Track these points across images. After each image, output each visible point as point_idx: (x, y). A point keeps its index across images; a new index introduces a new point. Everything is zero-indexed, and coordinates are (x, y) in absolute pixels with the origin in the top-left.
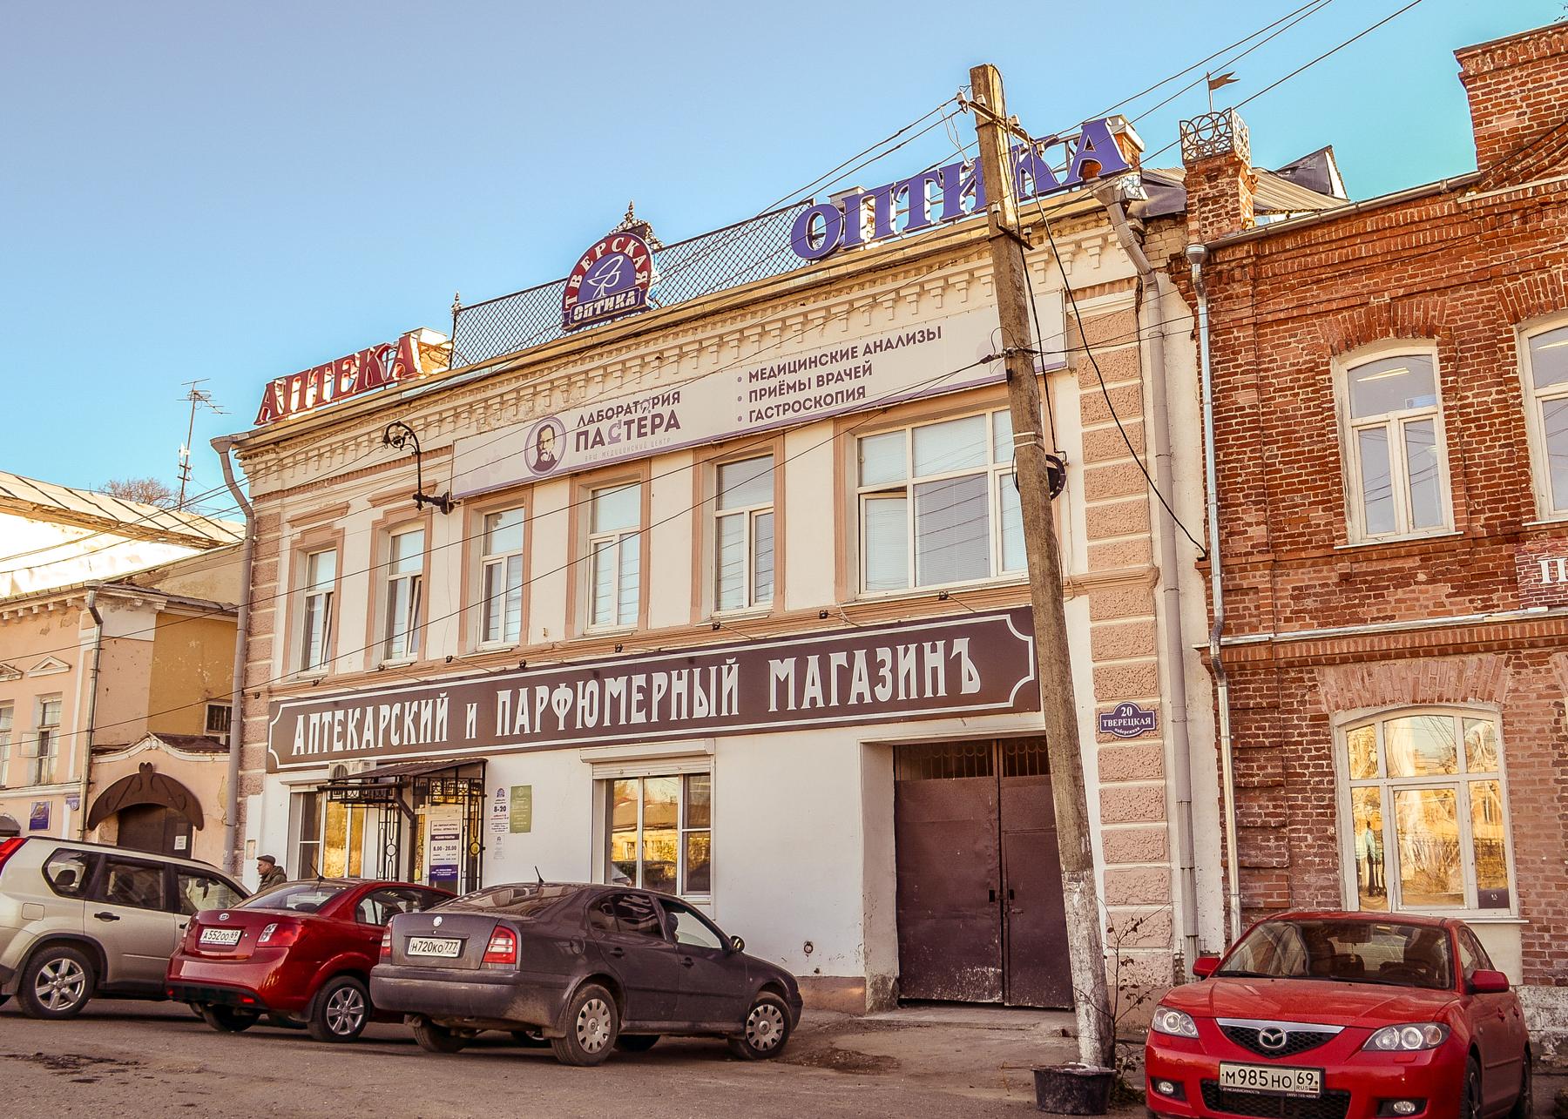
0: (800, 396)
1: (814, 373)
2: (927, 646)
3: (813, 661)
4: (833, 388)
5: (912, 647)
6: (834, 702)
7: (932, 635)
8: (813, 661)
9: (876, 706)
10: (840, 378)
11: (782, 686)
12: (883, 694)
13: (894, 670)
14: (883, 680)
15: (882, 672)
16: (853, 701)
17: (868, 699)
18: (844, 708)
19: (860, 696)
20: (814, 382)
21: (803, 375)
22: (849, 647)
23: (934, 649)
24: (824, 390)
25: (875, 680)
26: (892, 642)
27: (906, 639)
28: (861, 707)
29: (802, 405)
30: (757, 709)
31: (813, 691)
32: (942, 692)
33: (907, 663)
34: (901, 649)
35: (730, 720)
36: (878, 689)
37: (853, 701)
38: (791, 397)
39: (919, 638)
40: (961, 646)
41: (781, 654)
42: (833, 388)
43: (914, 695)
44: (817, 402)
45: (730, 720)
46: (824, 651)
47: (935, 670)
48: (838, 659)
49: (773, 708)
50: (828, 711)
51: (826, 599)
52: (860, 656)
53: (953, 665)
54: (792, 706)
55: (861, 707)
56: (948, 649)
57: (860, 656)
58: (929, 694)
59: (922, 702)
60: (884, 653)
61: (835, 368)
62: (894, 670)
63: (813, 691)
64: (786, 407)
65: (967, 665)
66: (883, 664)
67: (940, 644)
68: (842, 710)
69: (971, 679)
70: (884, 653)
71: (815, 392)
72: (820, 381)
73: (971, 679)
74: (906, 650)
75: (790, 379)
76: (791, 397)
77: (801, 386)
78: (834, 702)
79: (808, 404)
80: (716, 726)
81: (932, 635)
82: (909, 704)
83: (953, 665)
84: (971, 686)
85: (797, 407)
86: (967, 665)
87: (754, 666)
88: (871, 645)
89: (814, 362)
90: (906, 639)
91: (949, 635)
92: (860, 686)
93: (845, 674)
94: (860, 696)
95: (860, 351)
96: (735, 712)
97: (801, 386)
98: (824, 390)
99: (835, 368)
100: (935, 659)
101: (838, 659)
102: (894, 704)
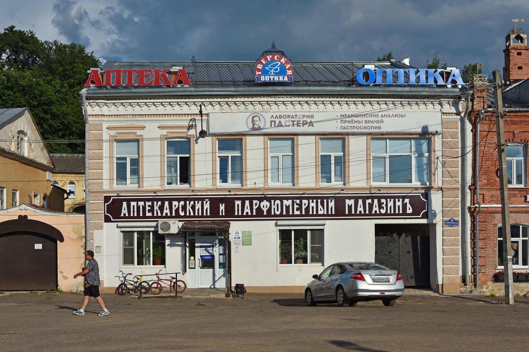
0: (360, 125)
3: (360, 202)
4: (370, 125)
5: (392, 200)
6: (367, 212)
7: (399, 197)
8: (360, 202)
9: (381, 214)
10: (372, 122)
11: (350, 207)
12: (383, 211)
13: (387, 205)
14: (383, 208)
15: (383, 205)
16: (373, 212)
17: (378, 212)
18: (370, 214)
19: (376, 211)
20: (364, 122)
21: (360, 119)
22: (373, 198)
23: (399, 201)
24: (367, 125)
25: (380, 207)
26: (386, 198)
27: (390, 197)
29: (360, 128)
30: (340, 213)
31: (360, 209)
32: (401, 212)
33: (391, 204)
34: (389, 200)
35: (332, 215)
36: (381, 210)
37: (373, 212)
38: (356, 125)
39: (394, 198)
40: (407, 201)
41: (350, 198)
42: (370, 125)
43: (392, 212)
44: (365, 128)
45: (332, 215)
46: (364, 199)
47: (399, 206)
49: (347, 213)
50: (365, 215)
51: (363, 184)
52: (376, 201)
53: (404, 206)
54: (353, 212)
55: (376, 214)
56: (403, 201)
57: (376, 201)
59: (395, 214)
60: (383, 201)
61: (371, 119)
62: (387, 205)
63: (360, 209)
64: (354, 127)
65: (408, 206)
66: (383, 203)
67: (401, 200)
68: (369, 215)
70: (383, 201)
71: (364, 125)
74: (390, 201)
76: (356, 125)
77: (360, 122)
78: (367, 212)
80: (327, 216)
83: (404, 206)
84: (410, 211)
86: (408, 206)
87: (340, 201)
88: (379, 198)
89: (364, 116)
90: (390, 197)
91: (404, 198)
92: (376, 209)
93: (371, 206)
94: (376, 211)
95: (380, 116)
96: (333, 213)
97: (360, 122)
98: (367, 125)
99: (371, 119)
100: (399, 203)
101: (370, 201)
102: (386, 214)
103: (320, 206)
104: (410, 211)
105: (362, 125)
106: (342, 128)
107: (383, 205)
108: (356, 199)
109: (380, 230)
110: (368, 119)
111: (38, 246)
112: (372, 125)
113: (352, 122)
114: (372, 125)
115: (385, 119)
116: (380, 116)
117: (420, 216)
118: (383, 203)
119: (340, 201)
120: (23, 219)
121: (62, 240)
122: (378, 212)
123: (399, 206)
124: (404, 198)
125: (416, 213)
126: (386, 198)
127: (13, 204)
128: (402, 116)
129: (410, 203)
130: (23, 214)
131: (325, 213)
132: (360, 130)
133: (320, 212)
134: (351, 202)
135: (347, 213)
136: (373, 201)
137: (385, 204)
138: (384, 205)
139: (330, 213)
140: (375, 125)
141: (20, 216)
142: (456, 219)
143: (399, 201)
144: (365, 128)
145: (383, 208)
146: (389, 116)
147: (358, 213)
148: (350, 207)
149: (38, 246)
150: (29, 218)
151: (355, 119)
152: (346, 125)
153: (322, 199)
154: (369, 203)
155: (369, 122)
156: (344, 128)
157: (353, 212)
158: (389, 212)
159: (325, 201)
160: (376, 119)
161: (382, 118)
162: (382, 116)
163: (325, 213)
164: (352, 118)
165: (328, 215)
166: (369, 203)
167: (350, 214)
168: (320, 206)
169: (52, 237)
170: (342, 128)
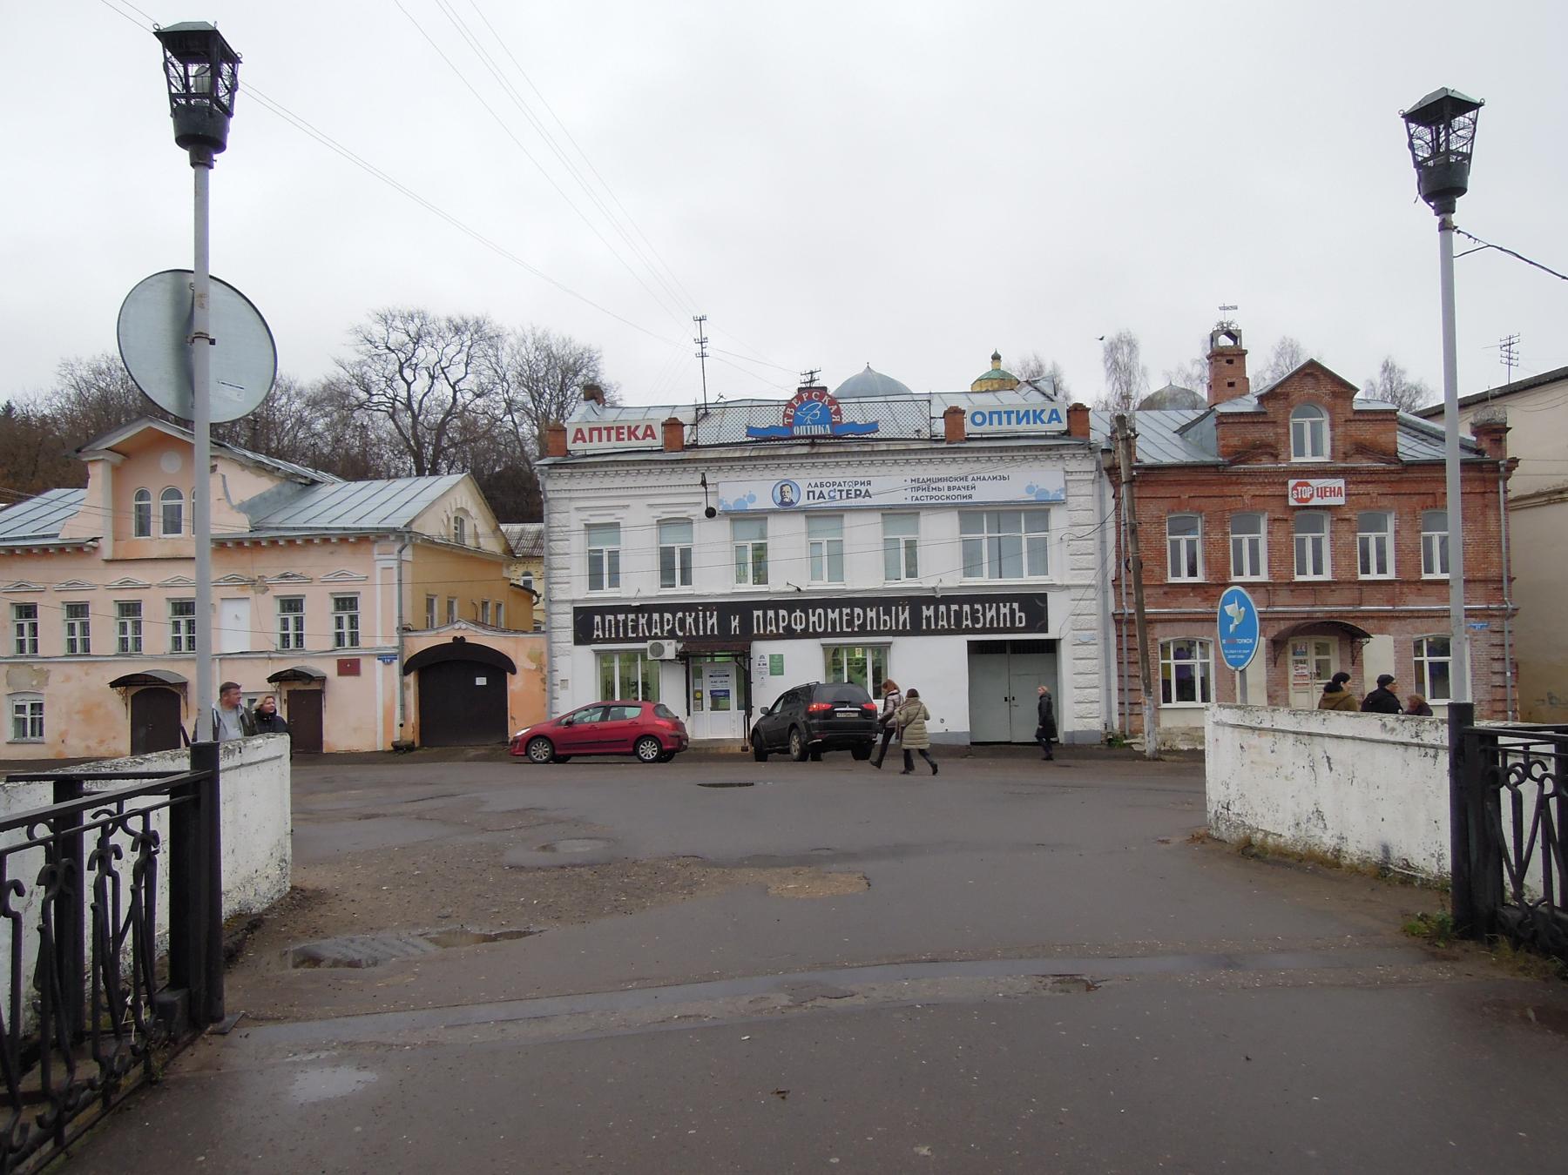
1: (946, 484)
4: (956, 492)
21: (940, 485)
24: (951, 493)
38: (934, 493)
40: (1016, 606)
42: (956, 492)
52: (966, 608)
53: (1012, 611)
62: (984, 615)
68: (959, 630)
76: (934, 493)
98: (951, 493)
100: (1005, 610)
105: (944, 494)
109: (975, 649)
111: (481, 681)
115: (977, 483)
120: (459, 641)
121: (514, 672)
127: (450, 621)
130: (459, 635)
141: (455, 638)
148: (928, 618)
149: (481, 681)
150: (469, 640)
152: (920, 493)
160: (965, 484)
169: (500, 666)
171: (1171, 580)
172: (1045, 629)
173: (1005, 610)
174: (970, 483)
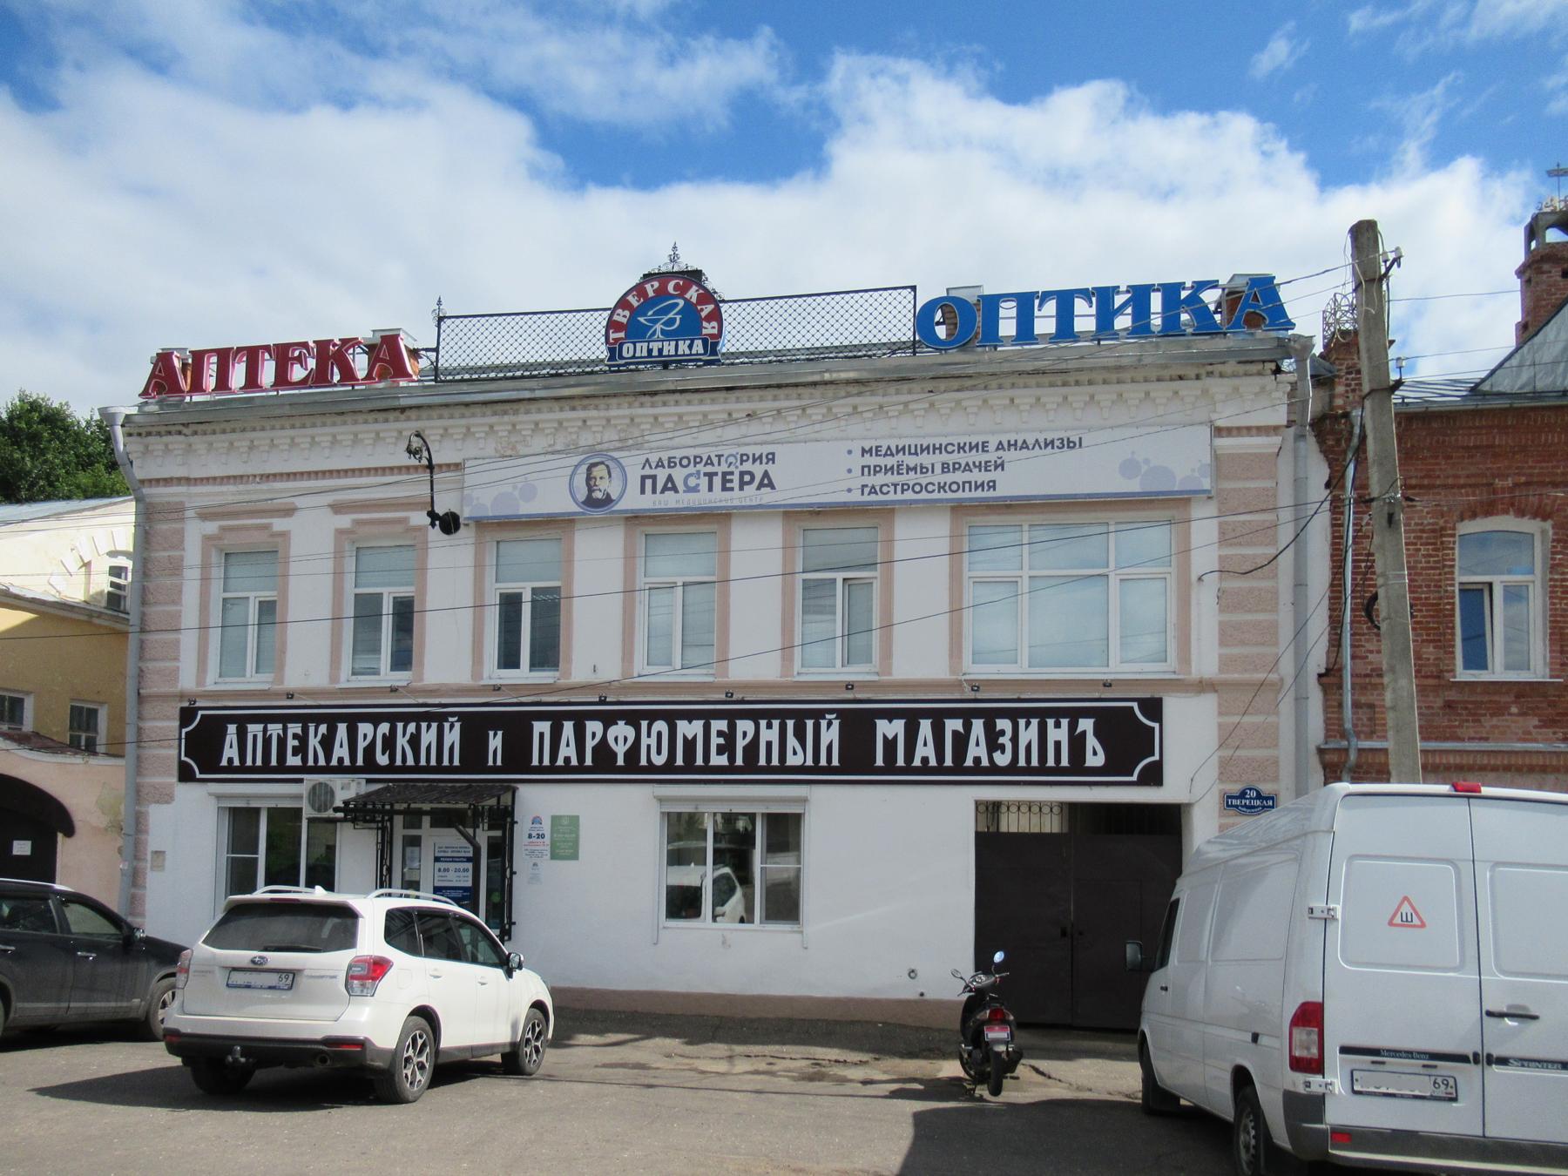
1: (938, 459)
2: (1051, 722)
3: (925, 726)
4: (959, 477)
5: (1035, 722)
6: (948, 762)
7: (1057, 714)
8: (925, 726)
9: (994, 769)
10: (967, 468)
11: (890, 745)
12: (1002, 759)
14: (1002, 748)
15: (1001, 740)
16: (969, 762)
17: (985, 763)
18: (958, 768)
19: (977, 760)
20: (938, 469)
21: (925, 459)
22: (967, 716)
23: (1058, 725)
24: (949, 478)
25: (993, 745)
26: (1013, 715)
28: (977, 768)
31: (925, 750)
32: (1065, 762)
33: (1029, 734)
34: (1022, 722)
36: (997, 756)
37: (969, 762)
38: (911, 478)
39: (1042, 714)
40: (1086, 725)
41: (890, 715)
42: (959, 477)
43: (1035, 762)
44: (941, 488)
46: (938, 718)
47: (1058, 744)
48: (953, 725)
49: (879, 762)
52: (978, 726)
53: (1077, 742)
54: (901, 762)
56: (1073, 727)
57: (978, 726)
58: (1051, 762)
59: (1042, 769)
60: (1003, 724)
61: (962, 458)
62: (1015, 740)
63: (925, 750)
64: (905, 488)
65: (1092, 742)
66: (1002, 733)
67: (1065, 722)
68: (957, 770)
69: (1095, 753)
70: (1003, 724)
72: (945, 468)
73: (1095, 753)
75: (911, 461)
76: (911, 478)
77: (923, 470)
78: (948, 762)
79: (930, 488)
81: (1057, 714)
82: (1029, 770)
83: (1077, 742)
84: (1096, 759)
85: (917, 488)
86: (1092, 742)
87: (858, 726)
88: (990, 717)
90: (1028, 714)
91: (1074, 715)
92: (977, 750)
93: (961, 741)
94: (977, 760)
97: (923, 470)
98: (949, 478)
99: (962, 458)
100: (1058, 734)
102: (1012, 768)
103: (792, 741)
104: (1096, 759)
106: (867, 490)
107: (1001, 740)
108: (911, 720)
110: (950, 459)
112: (967, 476)
113: (897, 469)
114: (967, 476)
115: (1007, 456)
116: (992, 446)
117: (1134, 778)
118: (1002, 733)
119: (858, 726)
122: (985, 763)
123: (1058, 744)
124: (1074, 715)
125: (1117, 765)
126: (1013, 715)
128: (1071, 445)
129: (1097, 734)
131: (810, 762)
132: (924, 495)
133: (792, 761)
134: (896, 728)
135: (879, 762)
136: (968, 727)
137: (1009, 734)
138: (1005, 740)
139: (823, 762)
140: (977, 476)
142: (1266, 789)
143: (1058, 725)
144: (941, 488)
145: (1002, 748)
146: (1025, 445)
147: (917, 762)
151: (911, 461)
153: (800, 717)
154: (955, 733)
155: (956, 467)
156: (873, 491)
157: (901, 762)
158: (1022, 762)
159: (810, 724)
160: (983, 457)
161: (1000, 453)
162: (1000, 447)
163: (810, 762)
164: (900, 457)
165: (816, 769)
166: (955, 733)
167: (890, 767)
168: (792, 741)
170: (867, 490)
171: (1463, 675)
172: (1153, 776)
173: (1058, 734)
174: (992, 456)
